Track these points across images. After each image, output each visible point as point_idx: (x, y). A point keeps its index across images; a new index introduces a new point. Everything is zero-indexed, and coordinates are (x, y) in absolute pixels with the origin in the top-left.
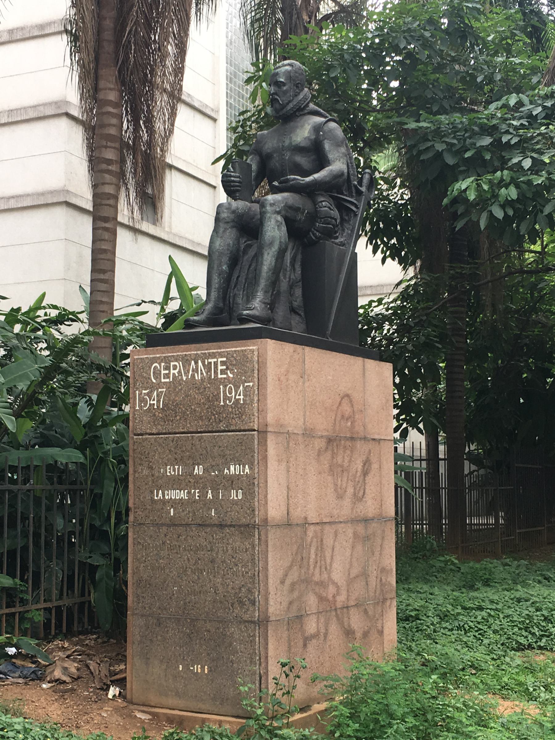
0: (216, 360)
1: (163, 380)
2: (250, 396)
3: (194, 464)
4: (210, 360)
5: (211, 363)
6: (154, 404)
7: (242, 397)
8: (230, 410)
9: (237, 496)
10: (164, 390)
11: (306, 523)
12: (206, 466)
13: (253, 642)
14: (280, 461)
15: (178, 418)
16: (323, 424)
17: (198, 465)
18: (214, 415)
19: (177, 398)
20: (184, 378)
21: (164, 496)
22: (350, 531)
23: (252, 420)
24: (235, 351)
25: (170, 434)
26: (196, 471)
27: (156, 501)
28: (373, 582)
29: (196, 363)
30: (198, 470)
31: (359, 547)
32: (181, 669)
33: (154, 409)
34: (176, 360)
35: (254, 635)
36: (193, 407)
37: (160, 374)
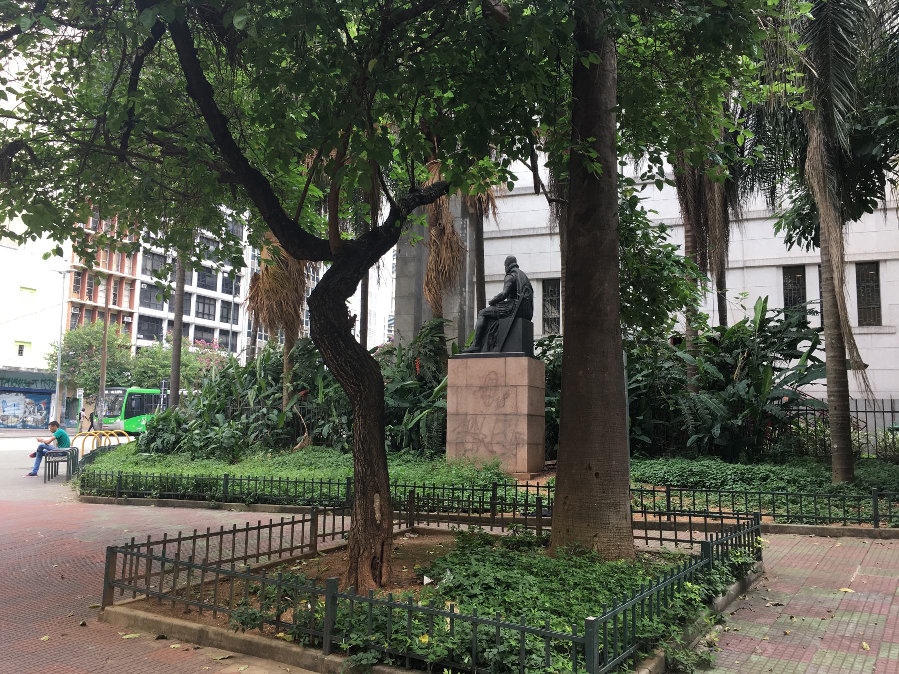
11: (466, 414)
14: (453, 395)
16: (477, 383)
22: (494, 418)
28: (510, 435)
31: (500, 424)
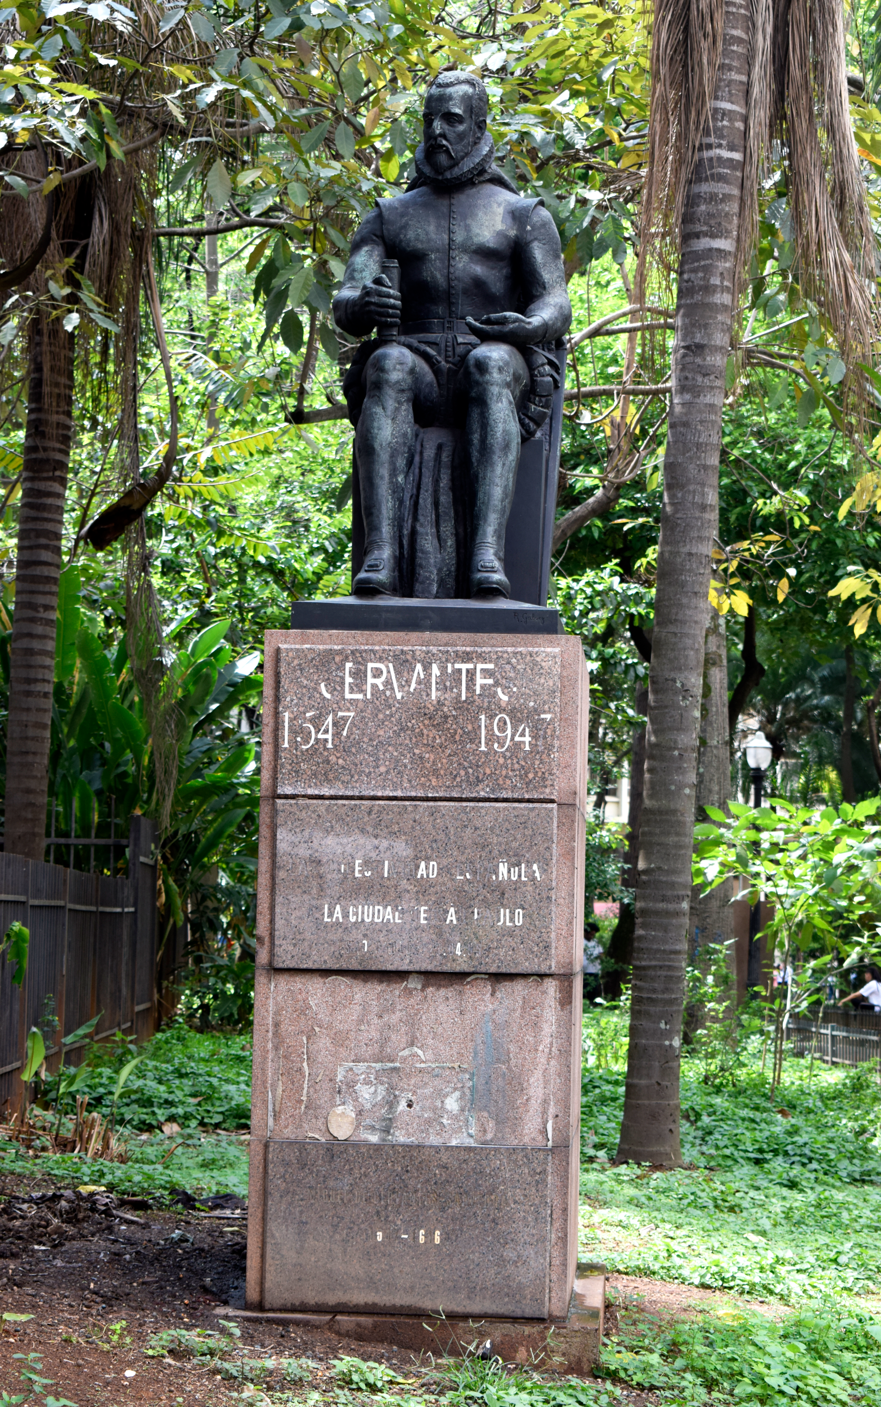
0: (470, 666)
1: (348, 696)
2: (545, 738)
3: (416, 858)
4: (457, 666)
5: (460, 671)
6: (326, 740)
7: (527, 739)
8: (501, 761)
9: (512, 920)
10: (352, 714)
12: (445, 862)
13: (541, 1183)
15: (383, 769)
17: (427, 859)
18: (465, 768)
19: (381, 733)
20: (399, 696)
21: (346, 915)
23: (549, 783)
24: (515, 653)
25: (361, 798)
26: (422, 871)
27: (326, 925)
29: (427, 667)
30: (428, 870)
32: (379, 1239)
33: (325, 749)
34: (380, 660)
35: (544, 1171)
36: (417, 751)
37: (343, 683)
